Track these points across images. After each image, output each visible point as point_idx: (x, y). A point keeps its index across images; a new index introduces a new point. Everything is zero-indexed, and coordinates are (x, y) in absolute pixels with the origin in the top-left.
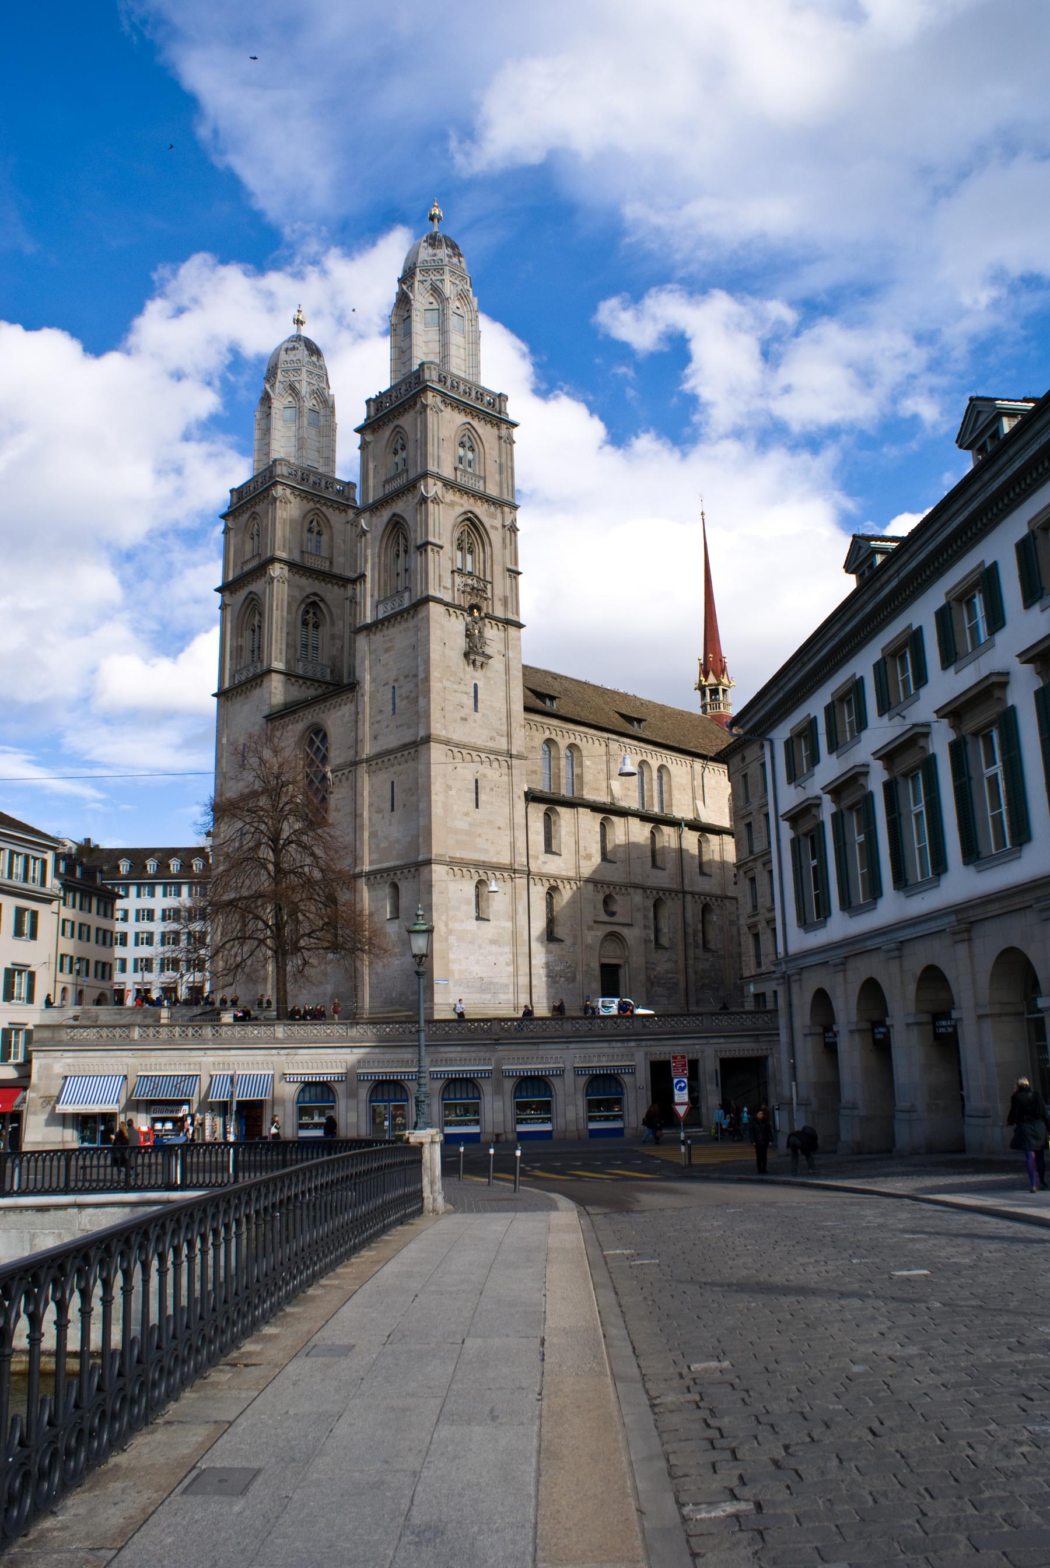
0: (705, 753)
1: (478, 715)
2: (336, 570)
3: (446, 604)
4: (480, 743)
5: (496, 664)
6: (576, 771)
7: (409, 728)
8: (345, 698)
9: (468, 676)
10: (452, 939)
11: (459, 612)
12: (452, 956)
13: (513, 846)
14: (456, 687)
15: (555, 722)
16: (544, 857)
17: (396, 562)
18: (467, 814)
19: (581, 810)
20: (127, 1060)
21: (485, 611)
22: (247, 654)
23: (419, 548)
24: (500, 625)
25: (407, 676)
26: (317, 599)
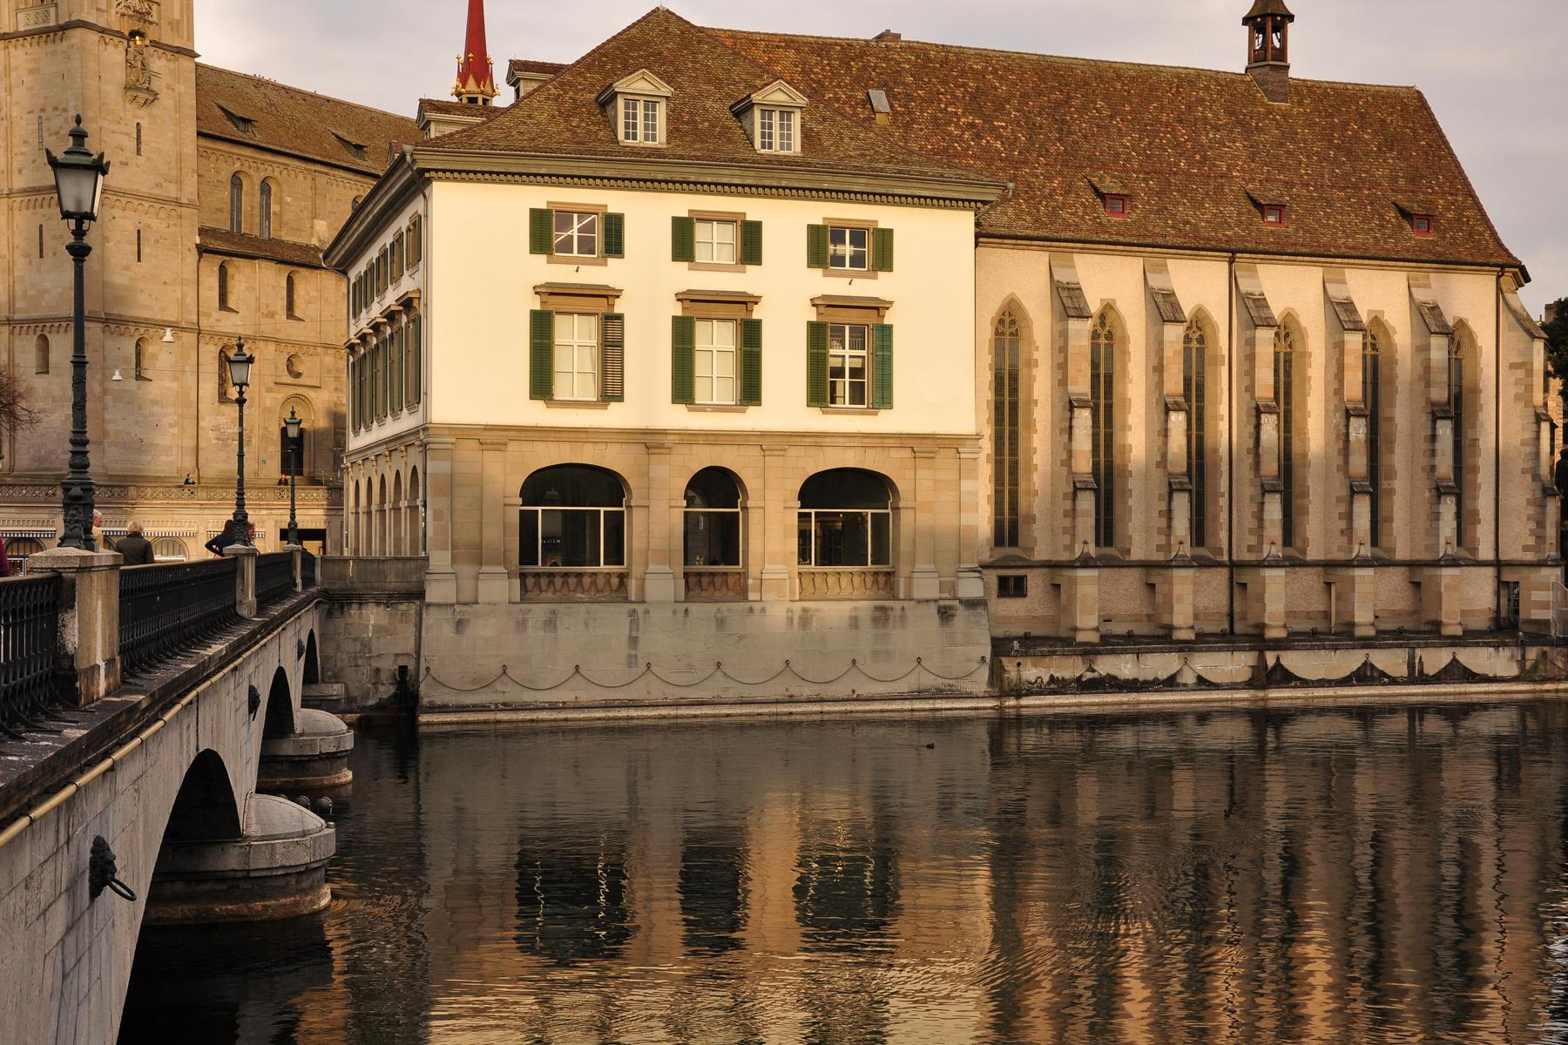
1: (141, 160)
3: (102, 31)
4: (143, 190)
5: (165, 99)
6: (274, 208)
9: (129, 115)
10: (108, 399)
11: (116, 40)
12: (108, 417)
13: (182, 303)
14: (113, 127)
15: (248, 152)
16: (218, 315)
18: (127, 268)
19: (264, 263)
25: (55, 109)
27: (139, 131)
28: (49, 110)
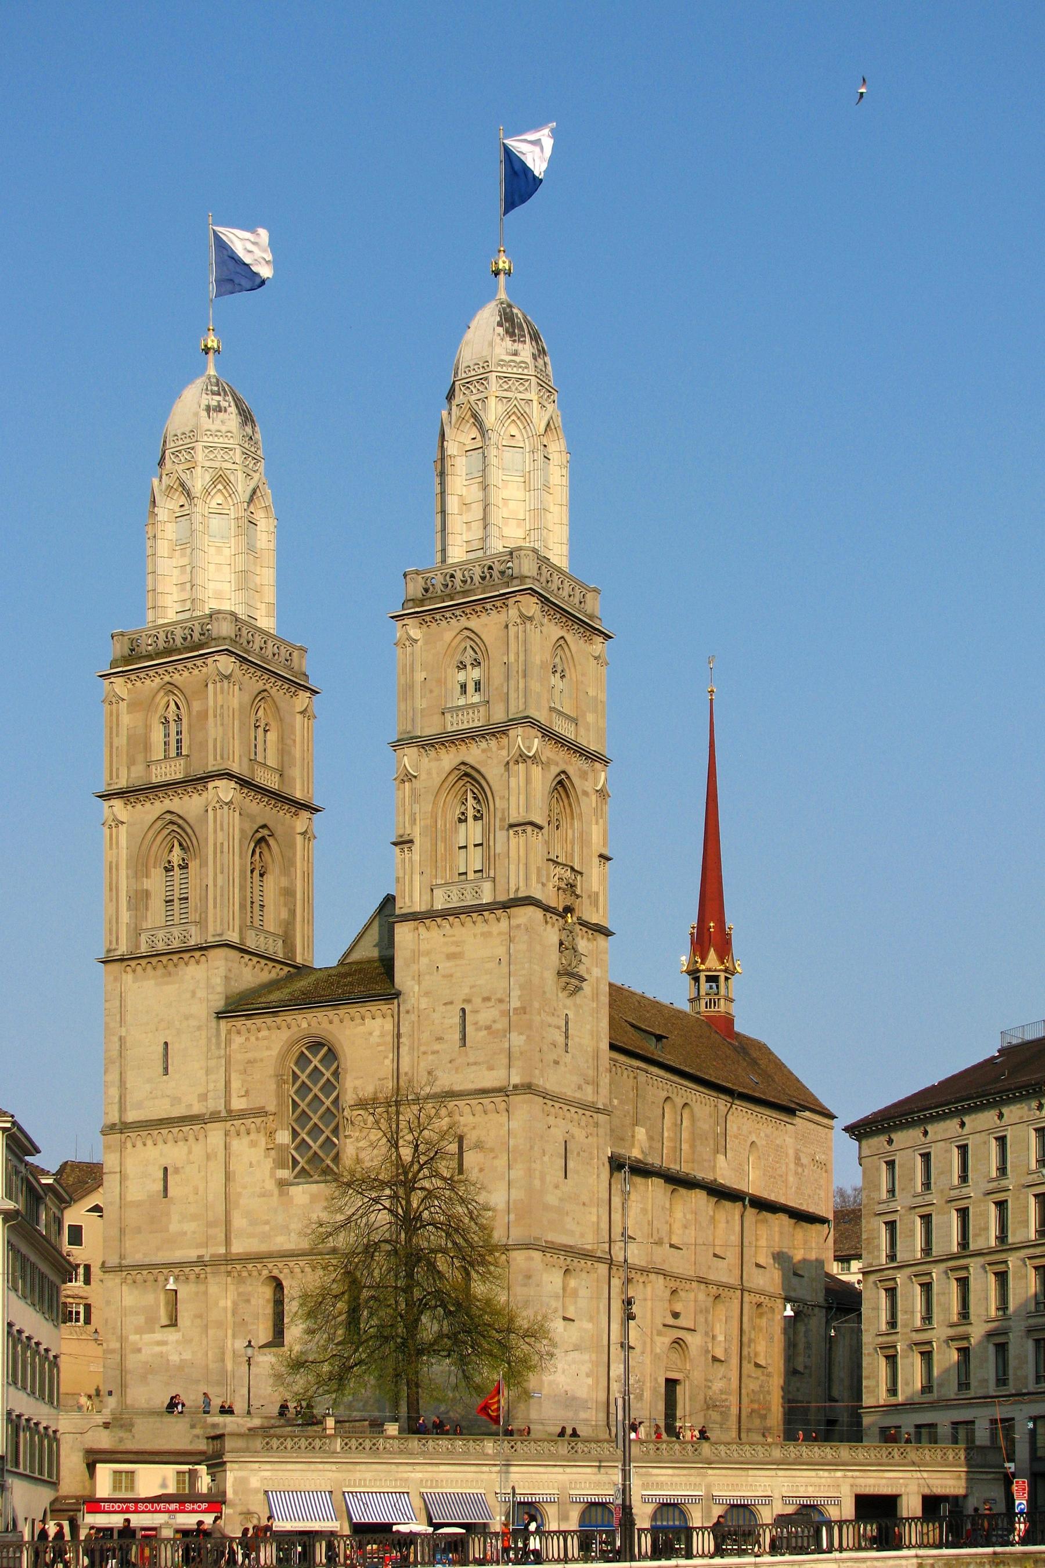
0: (729, 1085)
1: (569, 1055)
2: (287, 791)
4: (570, 1092)
7: (491, 1068)
8: (373, 1007)
11: (555, 917)
17: (457, 831)
18: (557, 1187)
20: (329, 1474)
21: (577, 914)
22: (157, 904)
23: (511, 826)
24: (590, 932)
25: (486, 999)
26: (265, 832)
27: (567, 1023)
28: (477, 1001)
